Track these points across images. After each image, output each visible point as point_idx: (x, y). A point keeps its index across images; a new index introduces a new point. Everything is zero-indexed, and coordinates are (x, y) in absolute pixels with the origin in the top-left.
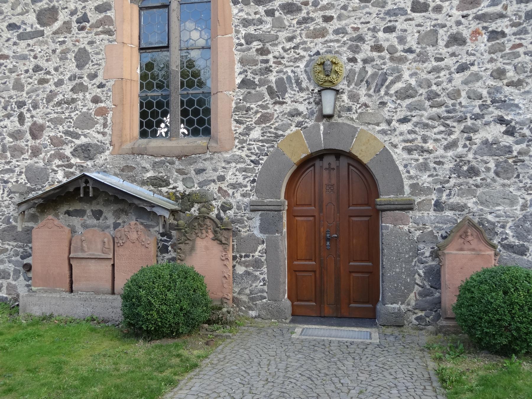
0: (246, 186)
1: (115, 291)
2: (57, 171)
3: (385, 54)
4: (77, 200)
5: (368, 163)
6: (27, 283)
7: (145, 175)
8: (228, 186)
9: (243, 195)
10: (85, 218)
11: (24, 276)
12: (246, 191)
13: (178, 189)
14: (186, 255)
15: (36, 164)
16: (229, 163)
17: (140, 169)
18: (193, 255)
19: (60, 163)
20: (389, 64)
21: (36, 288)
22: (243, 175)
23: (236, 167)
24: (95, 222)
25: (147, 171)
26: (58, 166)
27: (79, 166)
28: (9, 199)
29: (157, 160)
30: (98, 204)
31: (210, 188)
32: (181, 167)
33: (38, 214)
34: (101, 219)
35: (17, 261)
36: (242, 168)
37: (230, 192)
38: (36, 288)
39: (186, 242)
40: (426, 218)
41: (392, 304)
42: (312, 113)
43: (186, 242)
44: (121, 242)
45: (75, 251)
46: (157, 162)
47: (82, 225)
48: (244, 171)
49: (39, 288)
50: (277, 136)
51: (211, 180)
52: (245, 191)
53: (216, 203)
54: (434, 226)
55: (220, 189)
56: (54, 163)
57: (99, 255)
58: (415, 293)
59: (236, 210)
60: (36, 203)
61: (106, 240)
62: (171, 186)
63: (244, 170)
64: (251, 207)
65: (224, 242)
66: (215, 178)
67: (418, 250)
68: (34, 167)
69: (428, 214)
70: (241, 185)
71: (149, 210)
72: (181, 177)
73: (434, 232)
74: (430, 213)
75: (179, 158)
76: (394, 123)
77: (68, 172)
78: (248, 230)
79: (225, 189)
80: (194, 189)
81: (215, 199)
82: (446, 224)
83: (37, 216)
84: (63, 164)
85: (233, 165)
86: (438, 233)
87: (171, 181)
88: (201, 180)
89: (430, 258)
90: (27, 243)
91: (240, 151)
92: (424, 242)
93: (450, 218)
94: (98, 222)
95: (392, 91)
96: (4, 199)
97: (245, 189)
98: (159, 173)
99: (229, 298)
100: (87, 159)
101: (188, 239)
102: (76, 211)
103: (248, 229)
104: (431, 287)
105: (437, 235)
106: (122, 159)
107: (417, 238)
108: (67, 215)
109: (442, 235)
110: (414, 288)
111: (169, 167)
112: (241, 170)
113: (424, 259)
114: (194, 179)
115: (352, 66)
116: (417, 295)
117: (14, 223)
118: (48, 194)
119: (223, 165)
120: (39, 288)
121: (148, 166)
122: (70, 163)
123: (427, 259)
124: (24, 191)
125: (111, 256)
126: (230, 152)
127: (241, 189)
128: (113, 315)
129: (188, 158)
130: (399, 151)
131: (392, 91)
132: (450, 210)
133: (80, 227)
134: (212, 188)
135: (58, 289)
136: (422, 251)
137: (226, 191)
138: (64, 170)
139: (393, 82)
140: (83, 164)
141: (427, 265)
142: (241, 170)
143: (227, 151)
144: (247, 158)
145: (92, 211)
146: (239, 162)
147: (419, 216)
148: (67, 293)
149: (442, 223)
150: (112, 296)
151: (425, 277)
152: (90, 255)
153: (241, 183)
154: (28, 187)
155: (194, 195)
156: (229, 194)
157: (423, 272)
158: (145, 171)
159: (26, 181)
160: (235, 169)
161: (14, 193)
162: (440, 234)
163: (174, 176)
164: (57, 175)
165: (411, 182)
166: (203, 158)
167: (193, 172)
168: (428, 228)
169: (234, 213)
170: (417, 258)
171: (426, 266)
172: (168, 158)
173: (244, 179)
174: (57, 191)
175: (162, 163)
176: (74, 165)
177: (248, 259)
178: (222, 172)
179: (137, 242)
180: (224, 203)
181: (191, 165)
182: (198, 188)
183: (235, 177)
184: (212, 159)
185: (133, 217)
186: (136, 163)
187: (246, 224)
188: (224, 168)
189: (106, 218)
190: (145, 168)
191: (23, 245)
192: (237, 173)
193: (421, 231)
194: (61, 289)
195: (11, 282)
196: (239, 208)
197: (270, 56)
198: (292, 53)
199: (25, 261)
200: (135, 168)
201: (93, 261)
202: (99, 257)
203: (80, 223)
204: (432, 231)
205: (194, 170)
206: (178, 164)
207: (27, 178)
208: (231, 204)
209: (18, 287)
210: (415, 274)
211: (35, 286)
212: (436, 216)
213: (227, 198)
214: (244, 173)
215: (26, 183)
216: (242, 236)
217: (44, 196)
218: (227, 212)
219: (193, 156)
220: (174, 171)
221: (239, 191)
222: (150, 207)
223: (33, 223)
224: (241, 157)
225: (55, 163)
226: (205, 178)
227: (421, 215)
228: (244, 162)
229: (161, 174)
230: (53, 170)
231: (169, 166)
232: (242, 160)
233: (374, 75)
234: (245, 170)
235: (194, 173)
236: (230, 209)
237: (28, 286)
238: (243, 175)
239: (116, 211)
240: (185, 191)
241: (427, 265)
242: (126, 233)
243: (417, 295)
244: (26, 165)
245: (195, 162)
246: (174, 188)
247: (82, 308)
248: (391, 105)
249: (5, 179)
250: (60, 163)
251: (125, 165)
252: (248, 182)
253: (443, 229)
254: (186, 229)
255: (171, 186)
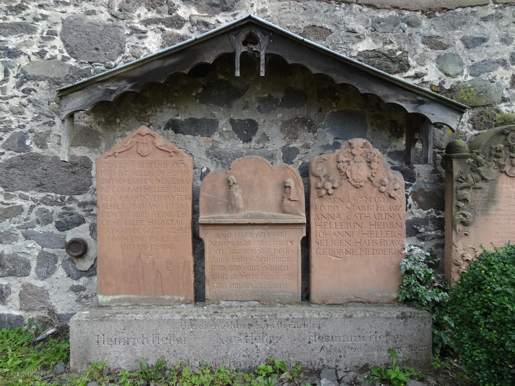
1: (314, 296)
2: (144, 32)
4: (196, 97)
6: (75, 283)
7: (354, 47)
10: (216, 137)
11: (66, 269)
13: (426, 79)
14: (475, 214)
15: (89, 18)
17: (343, 33)
18: (493, 212)
19: (153, 15)
21: (110, 298)
24: (240, 145)
25: (359, 38)
26: (147, 22)
27: (198, 22)
28: (21, 94)
29: (382, 15)
30: (246, 107)
31: (494, 78)
32: (434, 33)
33: (100, 129)
34: (254, 139)
35: (47, 235)
38: (110, 298)
39: (478, 185)
43: (478, 185)
44: (329, 185)
45: (211, 210)
46: (383, 20)
47: (208, 154)
49: (118, 297)
51: (498, 62)
53: (508, 108)
56: (135, 14)
57: (275, 217)
60: (112, 92)
61: (291, 182)
62: (411, 73)
66: (507, 57)
68: (85, 23)
71: (410, 111)
72: (433, 54)
77: (171, 35)
80: (461, 78)
81: (504, 100)
83: (97, 133)
84: (159, 16)
87: (412, 63)
88: (477, 59)
90: (71, 193)
94: (247, 145)
96: (9, 93)
98: (385, 43)
100: (217, 9)
101: (483, 179)
102: (193, 122)
106: (302, 10)
108: (171, 132)
111: (407, 33)
114: (464, 58)
117: (35, 149)
118: (145, 69)
120: (118, 297)
121: (360, 28)
122: (177, 16)
124: (62, 76)
125: (304, 221)
128: (323, 355)
129: (449, 13)
133: (204, 157)
134: (498, 78)
135: (167, 297)
138: (162, 30)
140: (207, 20)
145: (232, 121)
148: (191, 306)
150: (305, 308)
152: (252, 216)
154: (71, 68)
155: (462, 91)
158: (355, 39)
159: (66, 54)
161: (35, 78)
163: (420, 51)
164: (145, 41)
166: (482, 16)
167: (459, 44)
172: (407, 13)
174: (171, 61)
176: (185, 21)
179: (369, 185)
181: (455, 28)
182: (469, 78)
184: (500, 17)
185: (328, 135)
186: (333, 21)
189: (265, 138)
190: (353, 32)
191: (62, 199)
194: (176, 298)
195: (33, 282)
199: (70, 235)
200: (331, 32)
201: (257, 231)
202: (274, 221)
203: (204, 149)
205: (463, 40)
207: (66, 46)
209: (51, 293)
211: (105, 294)
215: (64, 59)
217: (135, 73)
219: (459, 10)
220: (418, 40)
222: (413, 102)
223: (87, 150)
225: (139, 16)
226: (486, 57)
229: (390, 47)
230: (135, 30)
231: (408, 30)
235: (462, 46)
237: (76, 289)
239: (290, 122)
240: (443, 82)
242: (341, 165)
244: (64, 16)
245: (464, 23)
246: (417, 76)
247: (243, 345)
249: (11, 47)
250: (153, 15)
251: (308, 23)
254: (480, 158)
255: (411, 73)
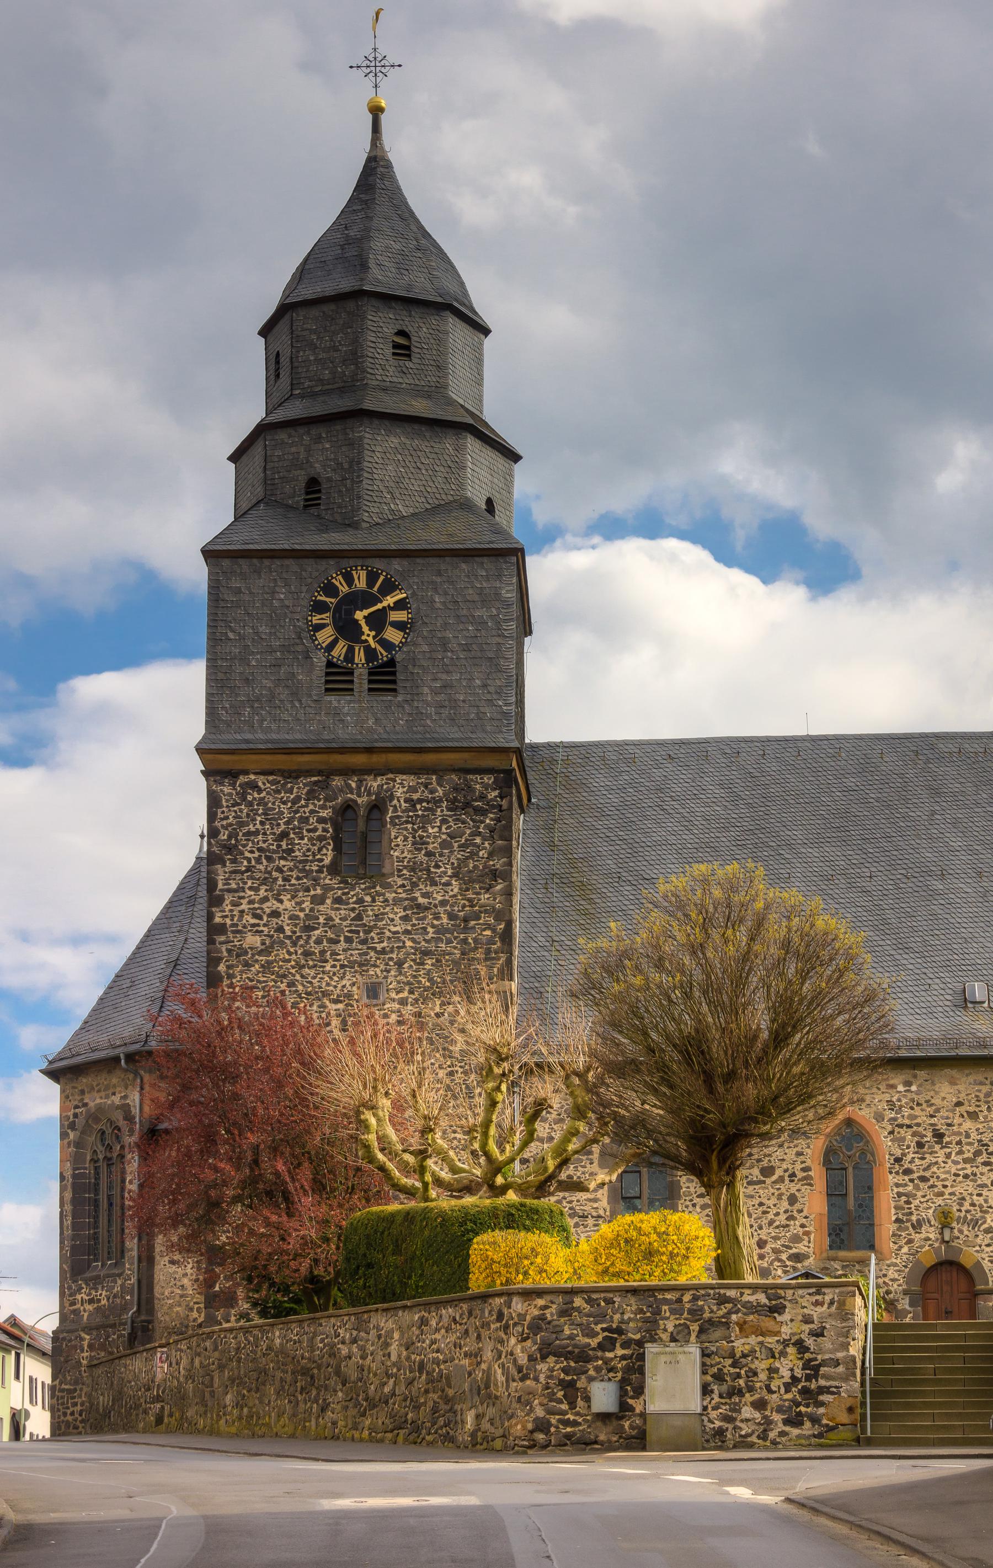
3: (977, 1208)
9: (899, 1285)
20: (980, 1214)
42: (937, 1239)
50: (917, 1252)
55: (884, 1282)
70: (897, 1280)
75: (858, 1262)
76: (983, 1247)
95: (982, 1229)
112: (896, 1271)
130: (986, 1262)
131: (982, 1229)
139: (982, 1224)
142: (896, 1271)
175: (847, 1266)
196: (896, 1293)
197: (912, 1206)
198: (925, 1204)
206: (857, 1267)
233: (972, 1220)
234: (899, 1271)
248: (981, 1237)
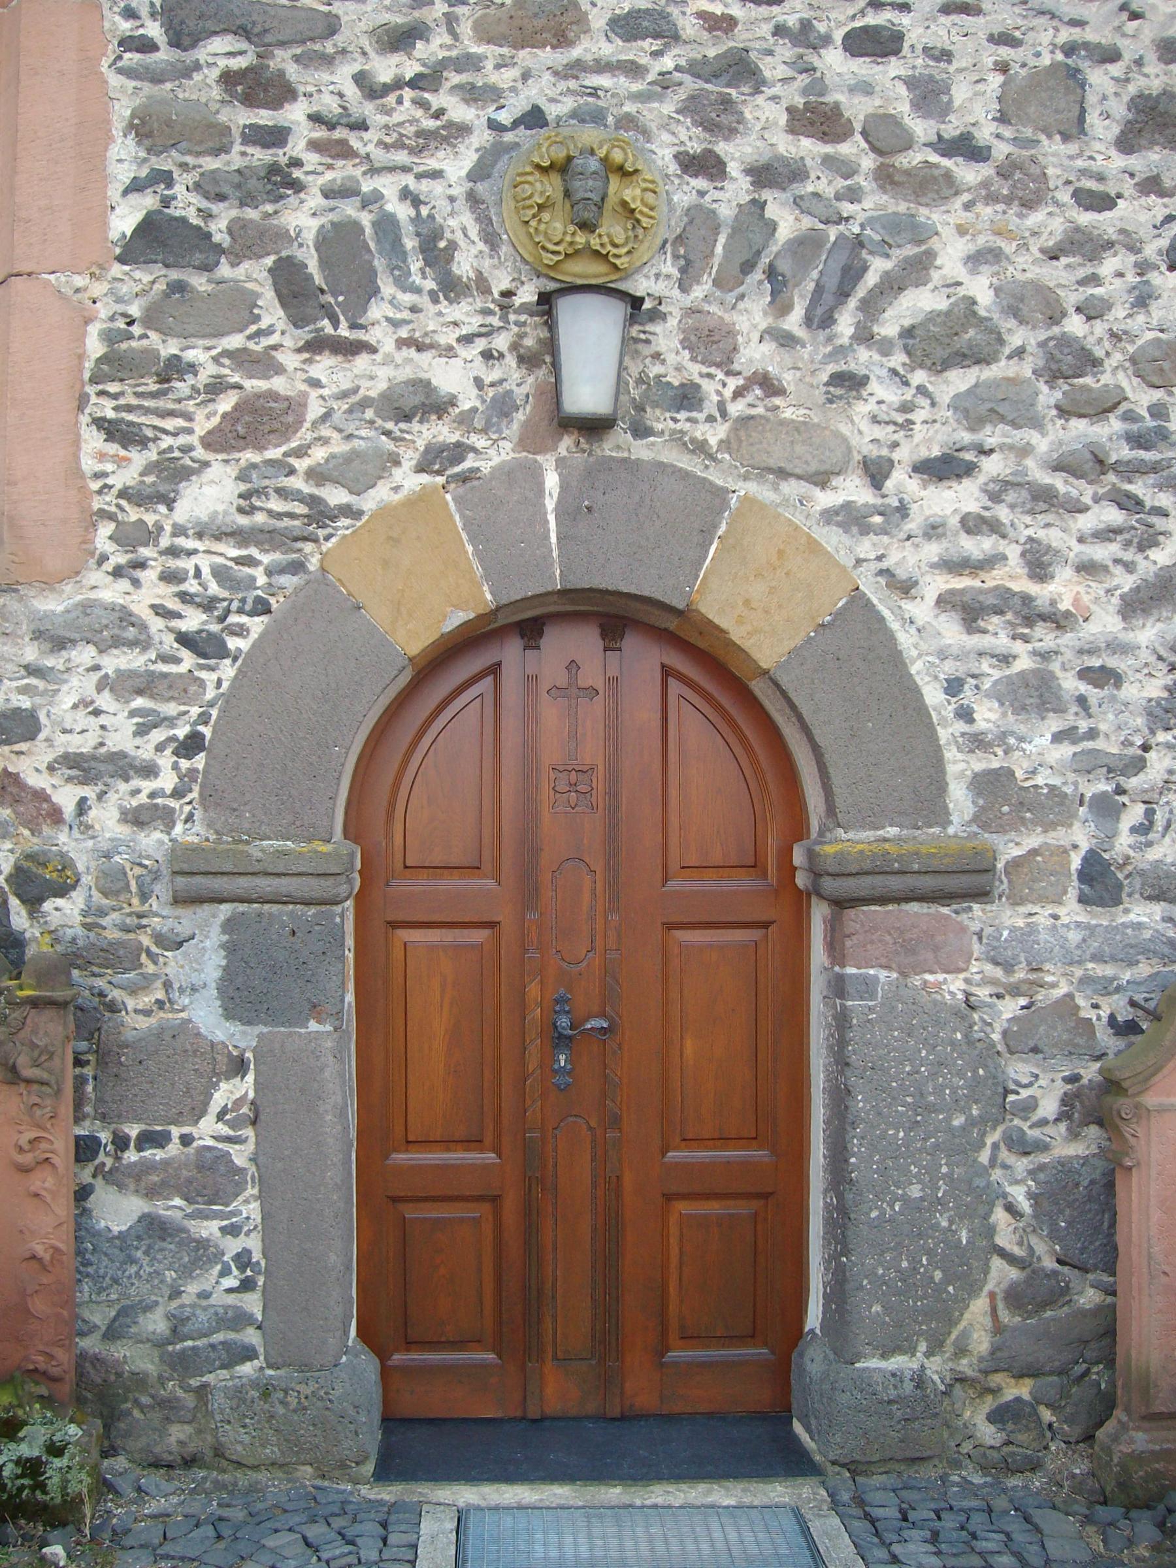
0: (150, 771)
3: (852, 148)
5: (780, 666)
8: (51, 768)
9: (137, 818)
12: (152, 795)
16: (60, 644)
20: (874, 201)
22: (133, 714)
23: (97, 668)
36: (132, 674)
37: (66, 797)
40: (1043, 936)
41: (884, 1356)
42: (503, 407)
48: (140, 692)
50: (321, 514)
52: (143, 798)
54: (1079, 973)
58: (992, 1296)
59: (96, 895)
63: (139, 683)
64: (181, 881)
65: (28, 1072)
67: (1007, 1092)
69: (1056, 917)
73: (1081, 1001)
74: (1061, 911)
76: (901, 481)
78: (160, 1004)
79: (35, 781)
82: (1133, 963)
85: (85, 655)
86: (1096, 1006)
89: (1063, 1127)
91: (124, 584)
92: (1035, 1050)
93: (1147, 934)
95: (889, 327)
97: (147, 786)
99: (55, 1371)
103: (160, 995)
104: (1059, 1261)
105: (1092, 1014)
107: (1005, 1033)
109: (1112, 1018)
110: (986, 1271)
113: (1034, 1133)
115: (701, 194)
116: (1001, 1305)
119: (31, 653)
123: (1049, 1130)
126: (68, 588)
127: (123, 787)
130: (922, 609)
131: (889, 327)
132: (1150, 898)
136: (1025, 1093)
137: (41, 796)
139: (892, 286)
141: (1045, 1159)
143: (49, 583)
144: (156, 624)
146: (117, 642)
147: (1013, 929)
149: (1114, 959)
151: (1036, 1216)
153: (122, 755)
156: (55, 816)
157: (1030, 1195)
160: (95, 676)
162: (1104, 1013)
165: (980, 763)
168: (1054, 985)
169: (85, 913)
170: (1000, 1130)
171: (1042, 1168)
173: (142, 731)
177: (158, 1154)
178: (25, 690)
180: (29, 857)
183: (94, 721)
187: (151, 968)
188: (32, 670)
192: (105, 701)
193: (1023, 1001)
197: (295, 114)
198: (405, 110)
204: (1070, 996)
208: (66, 864)
210: (992, 1205)
212: (1088, 927)
213: (46, 830)
214: (139, 702)
216: (129, 1035)
218: (48, 906)
221: (112, 797)
224: (126, 617)
227: (1021, 923)
228: (143, 643)
232: (131, 632)
233: (806, 245)
234: (146, 684)
236: (62, 891)
238: (133, 714)
241: (1045, 1159)
243: (1001, 1305)
248: (882, 391)
252: (160, 748)
253: (1118, 990)
